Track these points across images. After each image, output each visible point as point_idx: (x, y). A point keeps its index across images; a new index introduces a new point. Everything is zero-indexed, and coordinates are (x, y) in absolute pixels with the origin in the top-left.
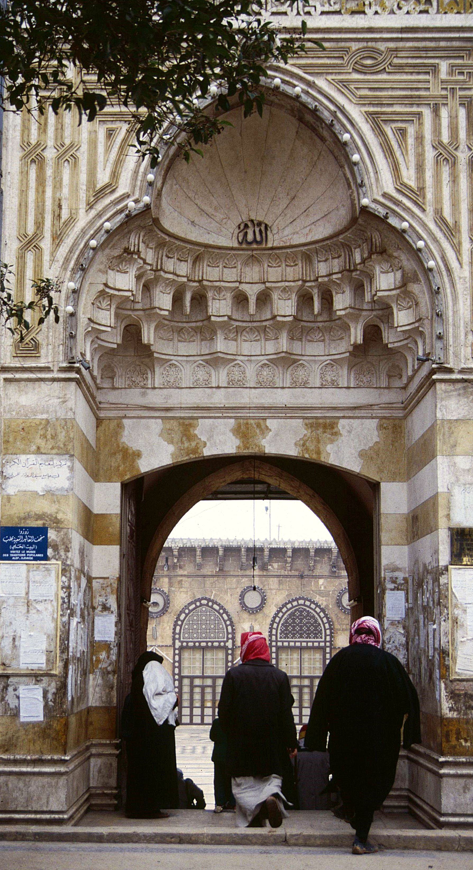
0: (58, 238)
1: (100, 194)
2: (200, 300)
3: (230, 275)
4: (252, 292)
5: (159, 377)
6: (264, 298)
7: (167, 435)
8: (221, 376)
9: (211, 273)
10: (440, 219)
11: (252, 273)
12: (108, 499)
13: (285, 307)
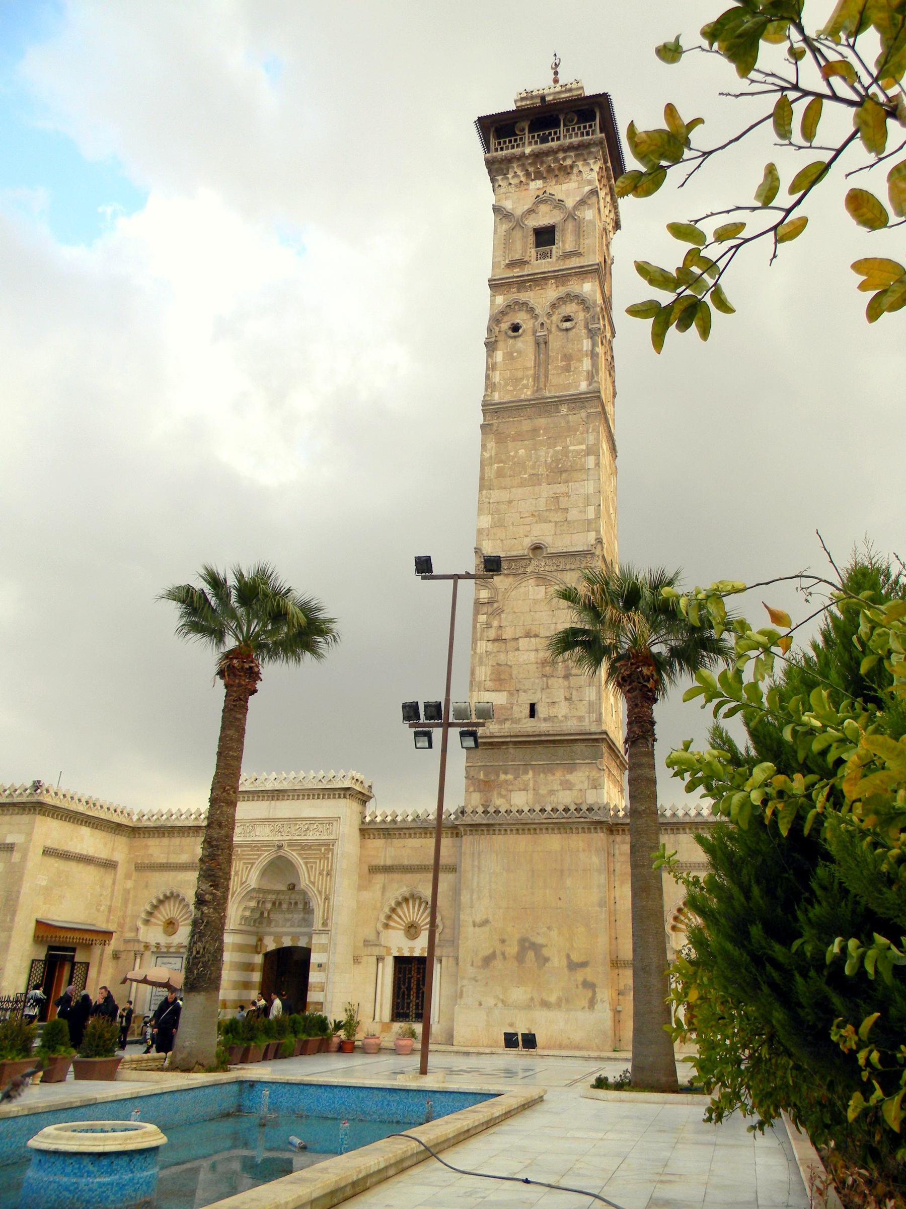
0: (232, 896)
1: (243, 884)
2: (280, 904)
3: (287, 897)
4: (293, 902)
5: (273, 924)
6: (296, 903)
7: (275, 941)
8: (288, 924)
9: (282, 897)
10: (318, 890)
11: (293, 896)
12: (259, 959)
13: (300, 906)
